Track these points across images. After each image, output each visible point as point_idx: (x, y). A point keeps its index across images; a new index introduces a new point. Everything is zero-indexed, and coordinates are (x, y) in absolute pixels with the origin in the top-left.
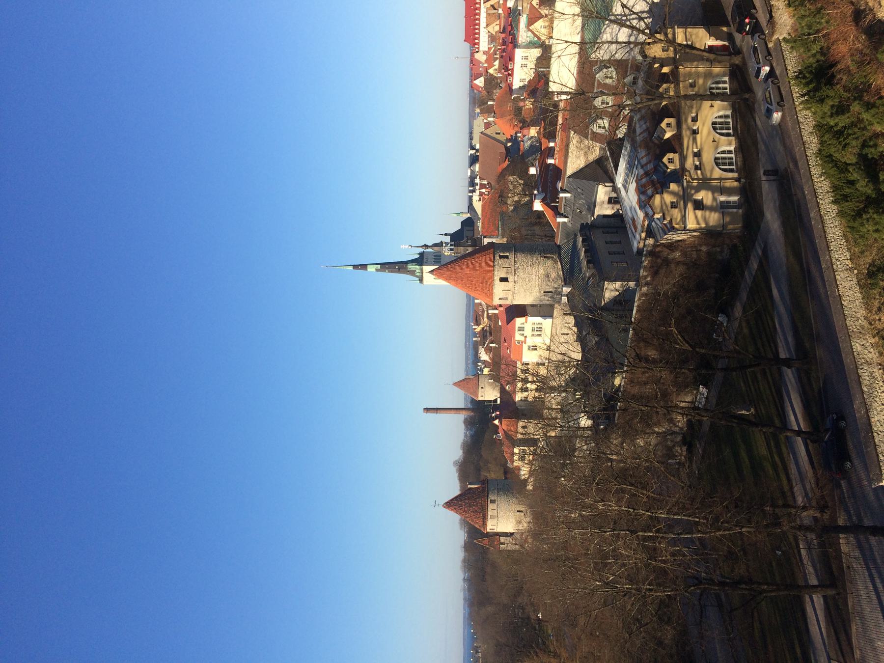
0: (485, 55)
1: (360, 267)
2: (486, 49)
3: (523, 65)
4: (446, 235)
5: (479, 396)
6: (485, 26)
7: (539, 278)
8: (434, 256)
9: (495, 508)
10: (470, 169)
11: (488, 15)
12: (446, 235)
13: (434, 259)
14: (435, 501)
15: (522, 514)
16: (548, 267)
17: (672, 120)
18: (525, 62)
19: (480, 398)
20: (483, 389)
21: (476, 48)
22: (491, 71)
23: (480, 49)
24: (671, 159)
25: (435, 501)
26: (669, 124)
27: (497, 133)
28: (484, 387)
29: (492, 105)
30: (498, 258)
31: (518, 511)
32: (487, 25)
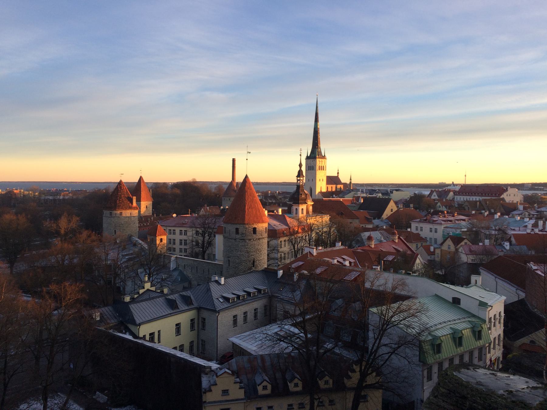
0: (451, 199)
1: (317, 117)
2: (455, 199)
3: (431, 229)
4: (338, 173)
5: (224, 198)
6: (468, 200)
7: (238, 257)
8: (323, 166)
9: (117, 215)
10: (377, 190)
11: (476, 202)
12: (338, 173)
13: (322, 166)
14: (123, 174)
15: (114, 233)
16: (246, 264)
17: (300, 388)
18: (433, 230)
19: (223, 198)
20: (229, 200)
21: (457, 193)
22: (439, 204)
23: (455, 196)
24: (266, 388)
25: (123, 174)
26: (297, 385)
27: (392, 210)
28: (230, 200)
29: (409, 207)
30: (254, 227)
31: (115, 231)
32: (469, 202)
